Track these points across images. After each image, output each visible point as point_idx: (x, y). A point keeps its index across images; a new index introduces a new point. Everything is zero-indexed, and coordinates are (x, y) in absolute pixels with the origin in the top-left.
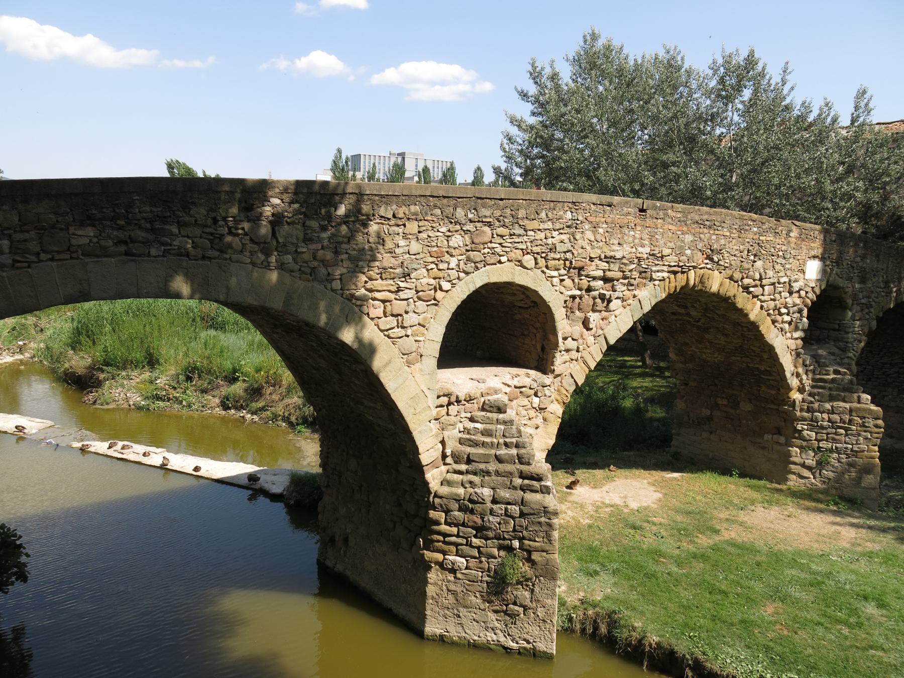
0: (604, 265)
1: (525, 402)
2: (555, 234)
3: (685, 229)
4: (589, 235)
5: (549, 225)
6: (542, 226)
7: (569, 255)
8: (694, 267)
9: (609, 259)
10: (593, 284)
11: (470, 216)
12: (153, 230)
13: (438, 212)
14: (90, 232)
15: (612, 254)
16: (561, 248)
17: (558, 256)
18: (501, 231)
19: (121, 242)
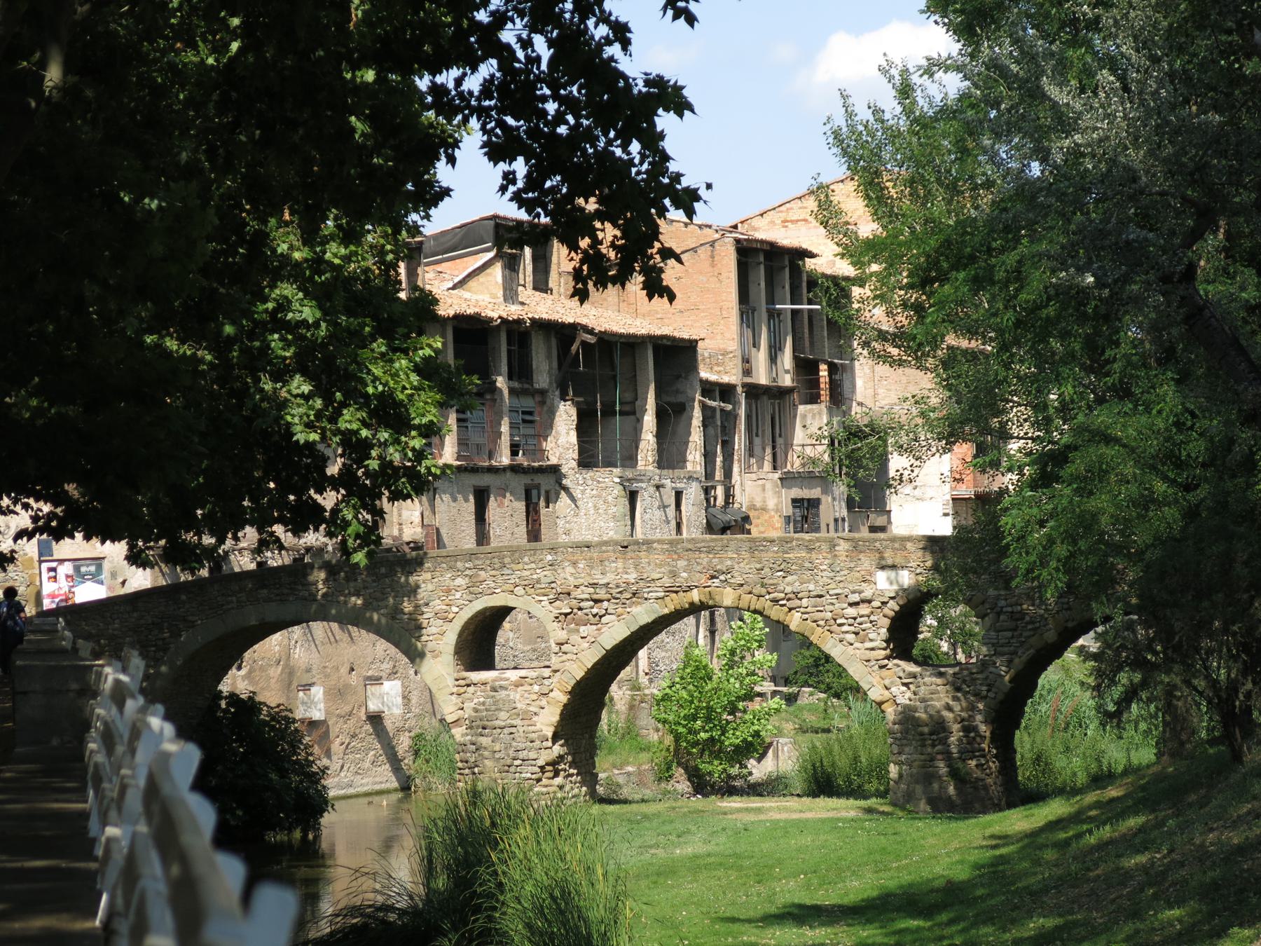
0: (591, 590)
1: (529, 688)
2: (538, 571)
3: (675, 557)
4: (570, 569)
5: (533, 566)
6: (526, 567)
7: (553, 585)
8: (696, 587)
9: (594, 585)
10: (583, 604)
11: (467, 565)
12: (291, 589)
13: (444, 565)
14: (265, 591)
15: (595, 581)
16: (544, 580)
17: (543, 586)
18: (493, 573)
19: (277, 595)
